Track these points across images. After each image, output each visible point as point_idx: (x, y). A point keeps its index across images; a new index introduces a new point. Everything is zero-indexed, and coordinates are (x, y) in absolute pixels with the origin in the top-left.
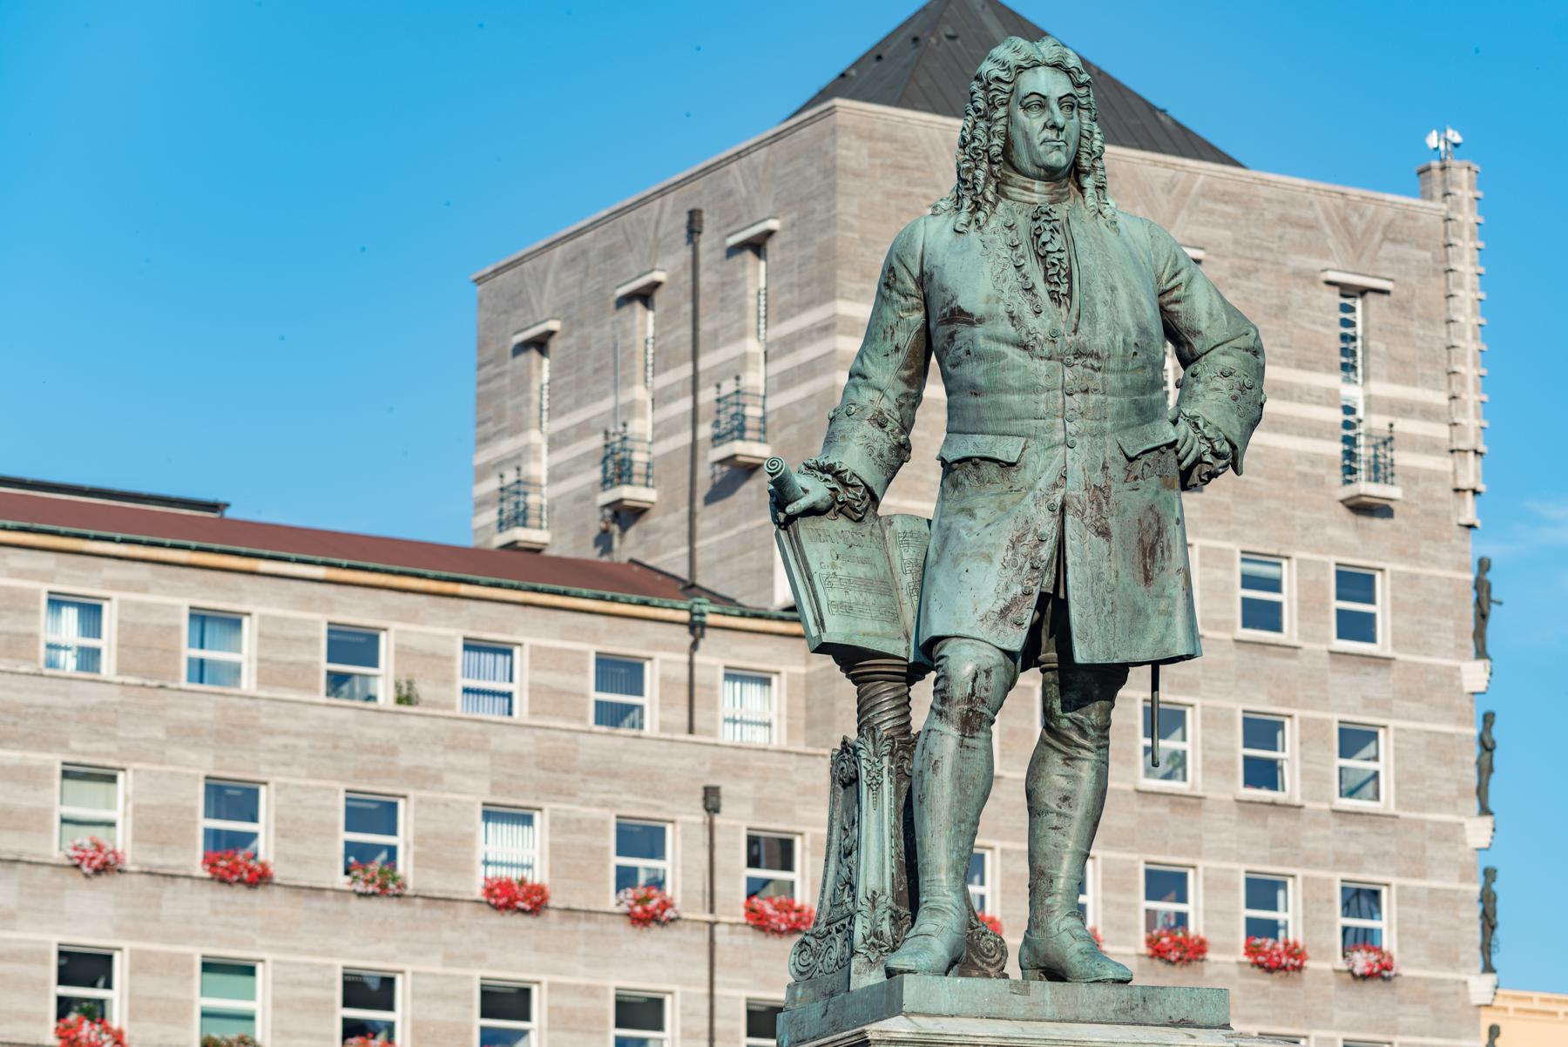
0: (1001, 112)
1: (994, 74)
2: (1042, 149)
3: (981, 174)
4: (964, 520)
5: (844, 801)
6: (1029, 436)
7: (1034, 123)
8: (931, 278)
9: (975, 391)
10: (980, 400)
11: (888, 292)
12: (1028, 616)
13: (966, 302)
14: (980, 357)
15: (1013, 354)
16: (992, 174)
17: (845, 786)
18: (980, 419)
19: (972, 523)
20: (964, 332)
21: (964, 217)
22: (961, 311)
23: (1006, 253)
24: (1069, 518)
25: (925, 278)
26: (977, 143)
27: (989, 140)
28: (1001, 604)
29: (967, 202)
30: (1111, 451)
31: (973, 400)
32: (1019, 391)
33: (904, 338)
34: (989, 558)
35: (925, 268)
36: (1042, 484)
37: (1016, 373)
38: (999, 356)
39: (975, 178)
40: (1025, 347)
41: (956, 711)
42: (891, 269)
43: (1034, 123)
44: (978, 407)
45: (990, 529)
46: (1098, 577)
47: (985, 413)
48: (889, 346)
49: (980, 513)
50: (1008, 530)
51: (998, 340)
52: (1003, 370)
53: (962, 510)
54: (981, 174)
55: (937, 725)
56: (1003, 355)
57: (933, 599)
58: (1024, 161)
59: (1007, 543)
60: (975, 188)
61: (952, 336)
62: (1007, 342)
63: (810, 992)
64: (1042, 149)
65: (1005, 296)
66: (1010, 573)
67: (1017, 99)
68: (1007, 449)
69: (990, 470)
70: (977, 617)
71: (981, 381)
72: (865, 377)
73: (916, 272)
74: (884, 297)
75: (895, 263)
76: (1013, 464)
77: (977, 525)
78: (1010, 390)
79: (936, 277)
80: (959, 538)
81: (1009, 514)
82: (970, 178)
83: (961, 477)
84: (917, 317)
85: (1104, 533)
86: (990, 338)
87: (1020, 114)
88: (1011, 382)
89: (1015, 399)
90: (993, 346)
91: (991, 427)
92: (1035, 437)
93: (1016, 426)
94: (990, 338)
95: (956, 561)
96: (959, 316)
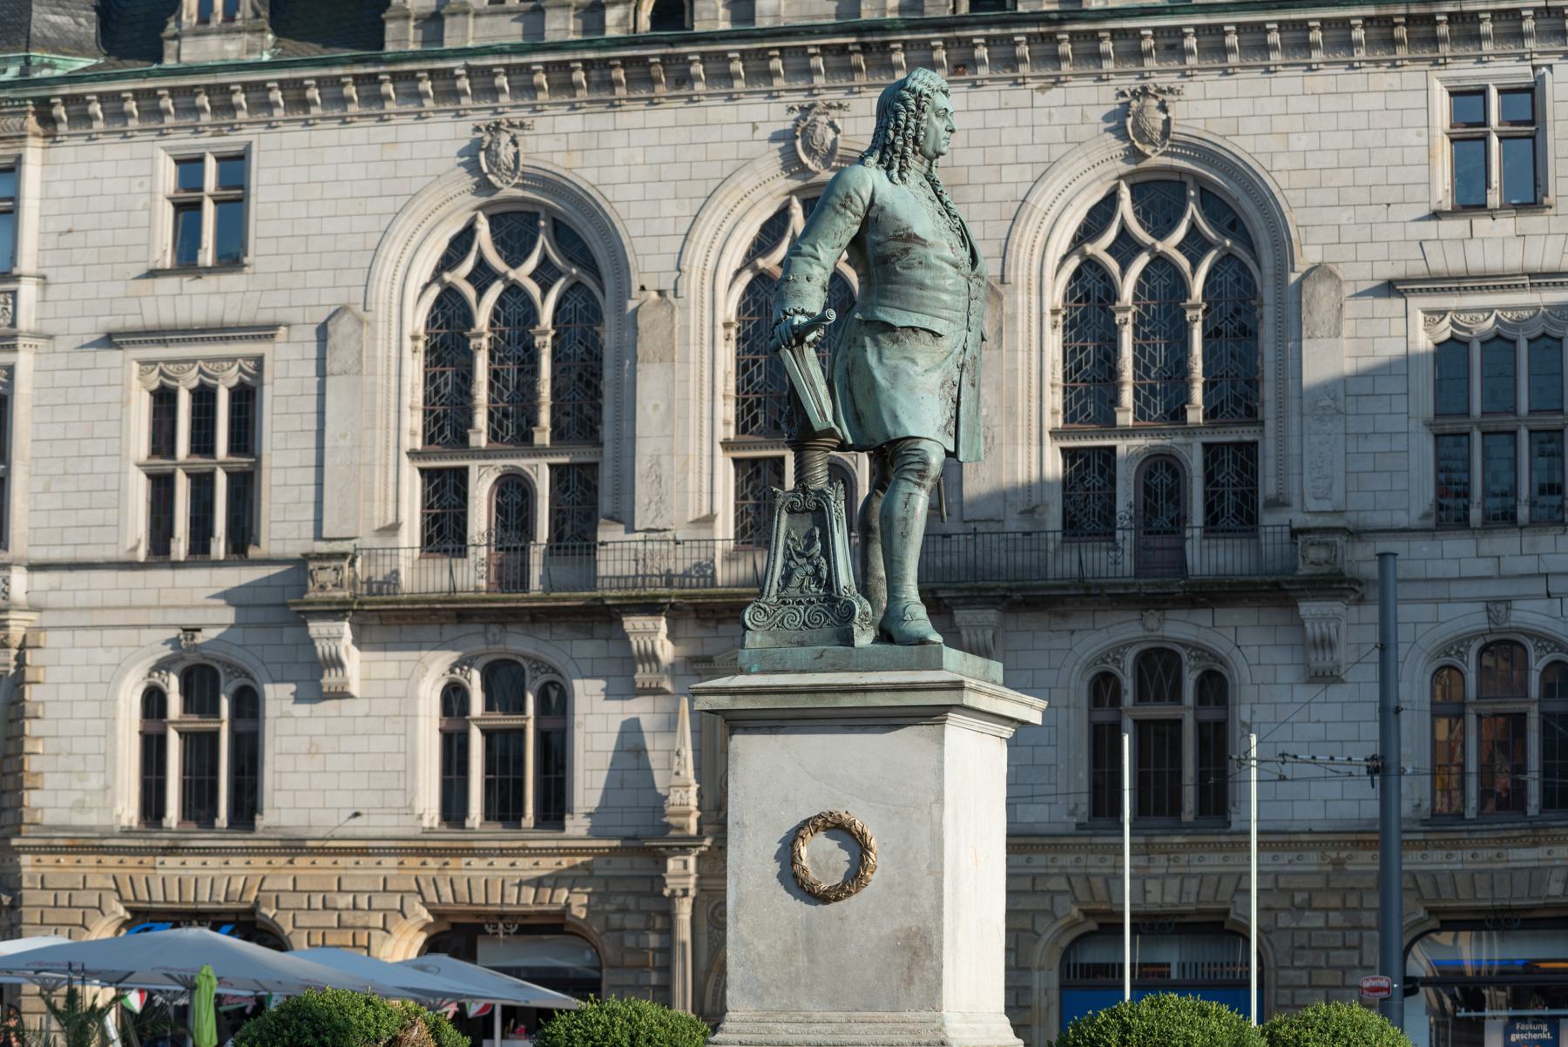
0: (925, 117)
1: (926, 91)
2: (943, 142)
3: (910, 150)
4: (903, 364)
5: (788, 521)
6: (951, 321)
7: (940, 125)
8: (882, 209)
9: (921, 286)
10: (924, 293)
11: (843, 210)
12: (953, 429)
13: (918, 230)
14: (929, 267)
15: (950, 270)
16: (914, 152)
17: (791, 511)
18: (922, 304)
19: (917, 369)
20: (918, 250)
21: (895, 172)
22: (917, 237)
23: (929, 203)
24: (964, 374)
25: (874, 208)
26: (910, 132)
27: (917, 131)
28: (945, 422)
29: (897, 165)
30: (979, 338)
31: (918, 292)
32: (952, 293)
33: (846, 240)
34: (930, 391)
35: (876, 201)
36: (957, 351)
37: (951, 281)
38: (940, 269)
39: (904, 151)
40: (956, 266)
41: (929, 483)
42: (848, 196)
43: (940, 125)
44: (922, 297)
45: (930, 374)
46: (968, 411)
47: (927, 302)
48: (837, 243)
49: (920, 361)
50: (935, 378)
51: (942, 259)
52: (944, 278)
53: (906, 358)
54: (910, 150)
55: (916, 490)
56: (945, 270)
57: (900, 412)
58: (929, 150)
59: (939, 384)
60: (903, 157)
61: (906, 251)
62: (947, 262)
63: (770, 639)
64: (943, 142)
65: (943, 232)
66: (944, 402)
67: (934, 109)
68: (938, 326)
69: (928, 336)
70: (935, 429)
71: (928, 282)
72: (818, 259)
73: (867, 202)
74: (838, 212)
75: (853, 193)
76: (940, 336)
77: (919, 369)
78: (946, 291)
79: (888, 209)
80: (908, 374)
81: (939, 366)
82: (899, 150)
83: (902, 337)
84: (856, 228)
85: (973, 385)
86: (938, 257)
87: (934, 118)
88: (950, 288)
89: (945, 297)
90: (938, 262)
91: (929, 311)
92: (954, 322)
93: (945, 313)
94: (938, 257)
95: (911, 389)
96: (912, 238)
